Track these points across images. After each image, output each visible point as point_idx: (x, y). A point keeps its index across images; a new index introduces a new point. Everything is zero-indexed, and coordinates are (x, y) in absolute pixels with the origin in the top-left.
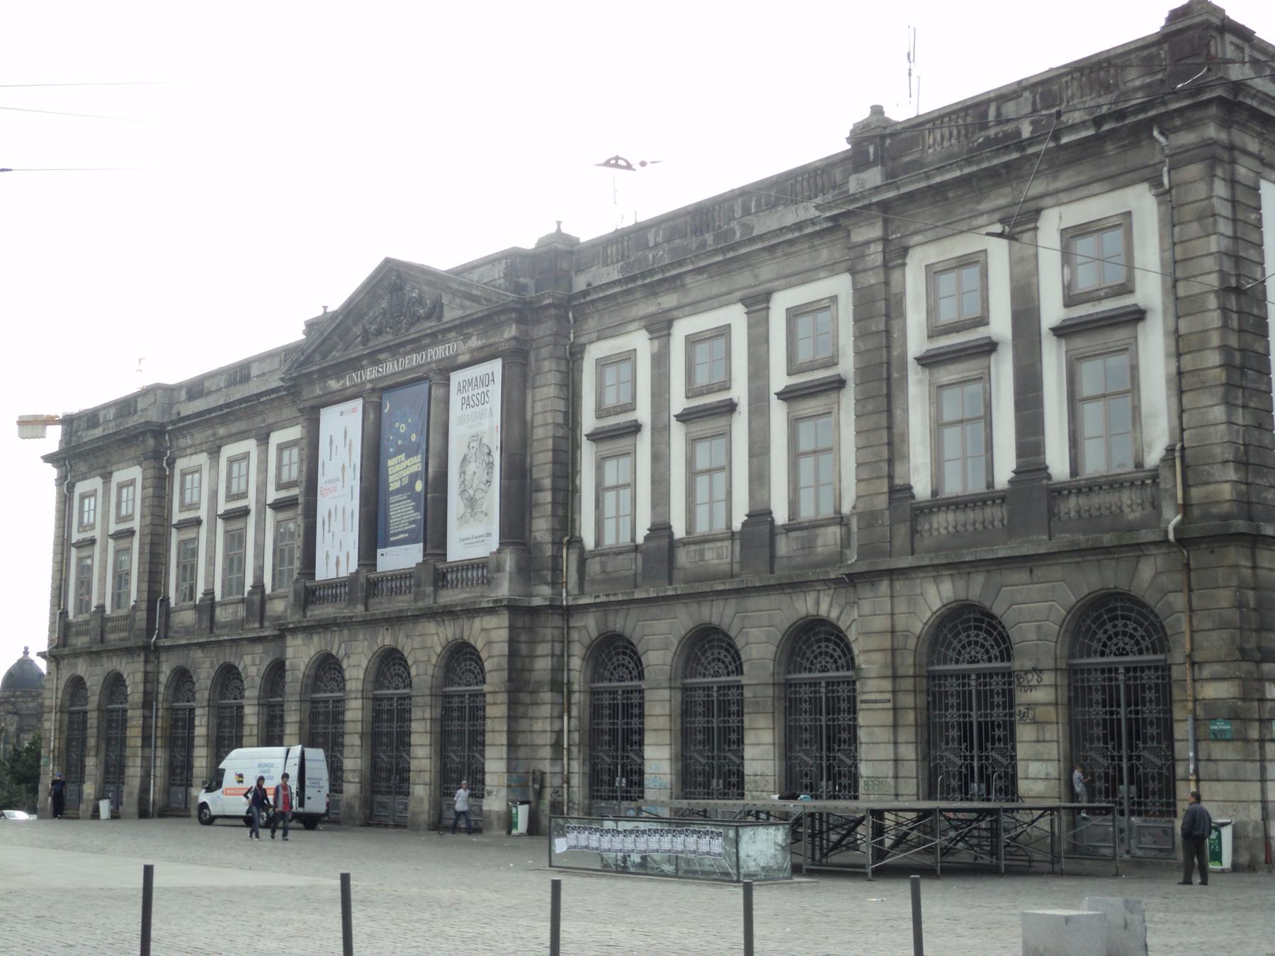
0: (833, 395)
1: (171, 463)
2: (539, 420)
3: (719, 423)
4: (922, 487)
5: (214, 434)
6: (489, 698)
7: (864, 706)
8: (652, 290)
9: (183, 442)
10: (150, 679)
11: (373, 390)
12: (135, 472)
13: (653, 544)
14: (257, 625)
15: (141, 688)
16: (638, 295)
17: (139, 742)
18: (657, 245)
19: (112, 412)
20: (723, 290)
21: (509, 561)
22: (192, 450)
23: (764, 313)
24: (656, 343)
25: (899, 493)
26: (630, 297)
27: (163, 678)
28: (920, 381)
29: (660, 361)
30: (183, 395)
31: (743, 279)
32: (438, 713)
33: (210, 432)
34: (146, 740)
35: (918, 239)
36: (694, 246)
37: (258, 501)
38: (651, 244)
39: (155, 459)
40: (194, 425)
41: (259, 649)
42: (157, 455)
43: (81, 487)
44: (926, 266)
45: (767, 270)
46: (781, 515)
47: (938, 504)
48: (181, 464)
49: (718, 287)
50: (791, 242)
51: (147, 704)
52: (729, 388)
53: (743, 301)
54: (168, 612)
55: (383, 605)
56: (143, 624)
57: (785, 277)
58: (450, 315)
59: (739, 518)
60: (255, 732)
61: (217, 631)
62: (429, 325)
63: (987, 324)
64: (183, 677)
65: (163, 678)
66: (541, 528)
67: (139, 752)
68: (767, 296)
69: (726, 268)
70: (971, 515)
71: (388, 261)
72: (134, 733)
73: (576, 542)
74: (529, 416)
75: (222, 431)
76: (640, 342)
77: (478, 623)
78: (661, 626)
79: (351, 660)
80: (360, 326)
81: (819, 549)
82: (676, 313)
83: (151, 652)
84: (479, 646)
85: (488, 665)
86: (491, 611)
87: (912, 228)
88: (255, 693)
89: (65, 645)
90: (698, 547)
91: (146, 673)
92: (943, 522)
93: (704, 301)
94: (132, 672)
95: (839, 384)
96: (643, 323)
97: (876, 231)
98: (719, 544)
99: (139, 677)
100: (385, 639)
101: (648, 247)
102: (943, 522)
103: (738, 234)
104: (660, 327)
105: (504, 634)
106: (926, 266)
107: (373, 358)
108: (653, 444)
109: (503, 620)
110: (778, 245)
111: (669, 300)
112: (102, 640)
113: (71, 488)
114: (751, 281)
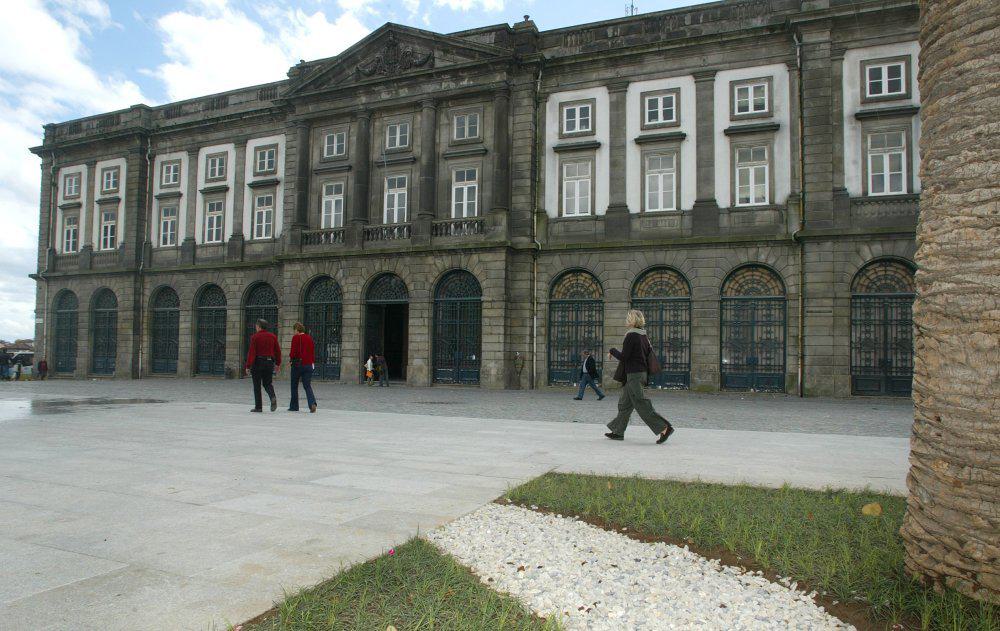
0: (768, 135)
1: (152, 158)
2: (518, 135)
3: (673, 145)
4: (854, 187)
5: (193, 140)
6: (484, 305)
7: (809, 314)
8: (614, 62)
9: (162, 145)
10: (138, 293)
11: (367, 110)
12: (122, 163)
13: (613, 215)
14: (238, 260)
15: (132, 298)
16: (601, 65)
17: (131, 332)
18: (614, 37)
19: (95, 123)
20: (676, 66)
21: (503, 218)
22: (173, 150)
23: (709, 83)
24: (615, 96)
25: (840, 193)
26: (595, 66)
27: (148, 293)
28: (854, 128)
29: (618, 109)
30: (162, 113)
31: (694, 61)
32: (432, 315)
33: (190, 138)
34: (137, 330)
35: (853, 45)
36: (649, 39)
37: (236, 182)
38: (610, 34)
39: (141, 153)
40: (175, 133)
41: (240, 274)
42: (143, 151)
43: (65, 171)
44: (861, 62)
45: (714, 58)
46: (723, 202)
47: (864, 200)
48: (159, 159)
49: (669, 65)
50: (740, 41)
51: (137, 308)
52: (679, 126)
53: (695, 75)
54: (151, 250)
55: (374, 246)
56: (133, 257)
57: (730, 63)
58: (439, 64)
59: (688, 204)
60: (237, 325)
61: (197, 264)
62: (425, 69)
63: (910, 98)
64: (166, 293)
65: (148, 293)
66: (521, 201)
67: (131, 338)
68: (714, 73)
69: (681, 53)
70: (895, 207)
71: (389, 25)
72: (125, 328)
73: (542, 213)
74: (510, 132)
75: (200, 138)
76: (601, 96)
77: (475, 257)
78: (624, 265)
79: (350, 280)
80: (354, 69)
81: (757, 224)
82: (633, 78)
83: (138, 276)
84: (476, 272)
85: (484, 284)
86: (491, 249)
87: (850, 38)
88: (238, 302)
89: (54, 271)
90: (651, 219)
91: (135, 288)
92: (868, 210)
93: (658, 72)
94: (123, 290)
95: (775, 128)
96: (601, 83)
97: (826, 36)
98: (671, 218)
99: (130, 291)
100: (379, 266)
101: (606, 37)
102: (868, 210)
103: (688, 34)
104: (618, 88)
105: (501, 265)
106: (861, 62)
107: (369, 89)
108: (611, 156)
109: (502, 256)
110: (721, 41)
111: (624, 70)
112: (91, 268)
113: (57, 170)
114: (701, 63)
